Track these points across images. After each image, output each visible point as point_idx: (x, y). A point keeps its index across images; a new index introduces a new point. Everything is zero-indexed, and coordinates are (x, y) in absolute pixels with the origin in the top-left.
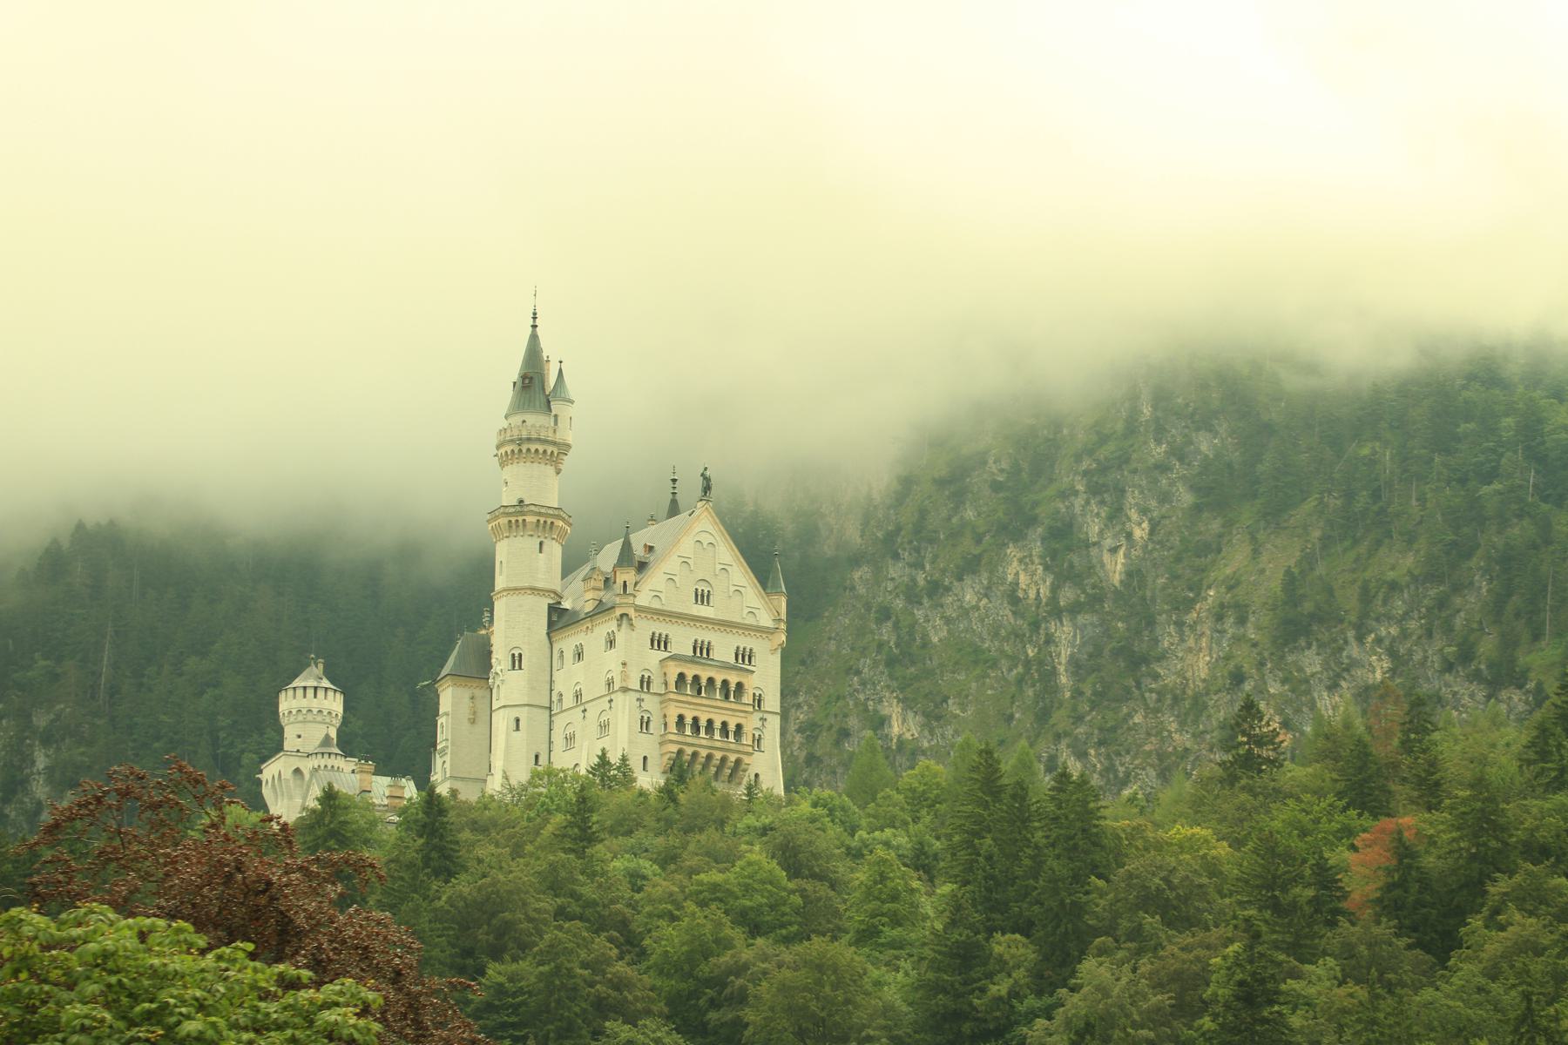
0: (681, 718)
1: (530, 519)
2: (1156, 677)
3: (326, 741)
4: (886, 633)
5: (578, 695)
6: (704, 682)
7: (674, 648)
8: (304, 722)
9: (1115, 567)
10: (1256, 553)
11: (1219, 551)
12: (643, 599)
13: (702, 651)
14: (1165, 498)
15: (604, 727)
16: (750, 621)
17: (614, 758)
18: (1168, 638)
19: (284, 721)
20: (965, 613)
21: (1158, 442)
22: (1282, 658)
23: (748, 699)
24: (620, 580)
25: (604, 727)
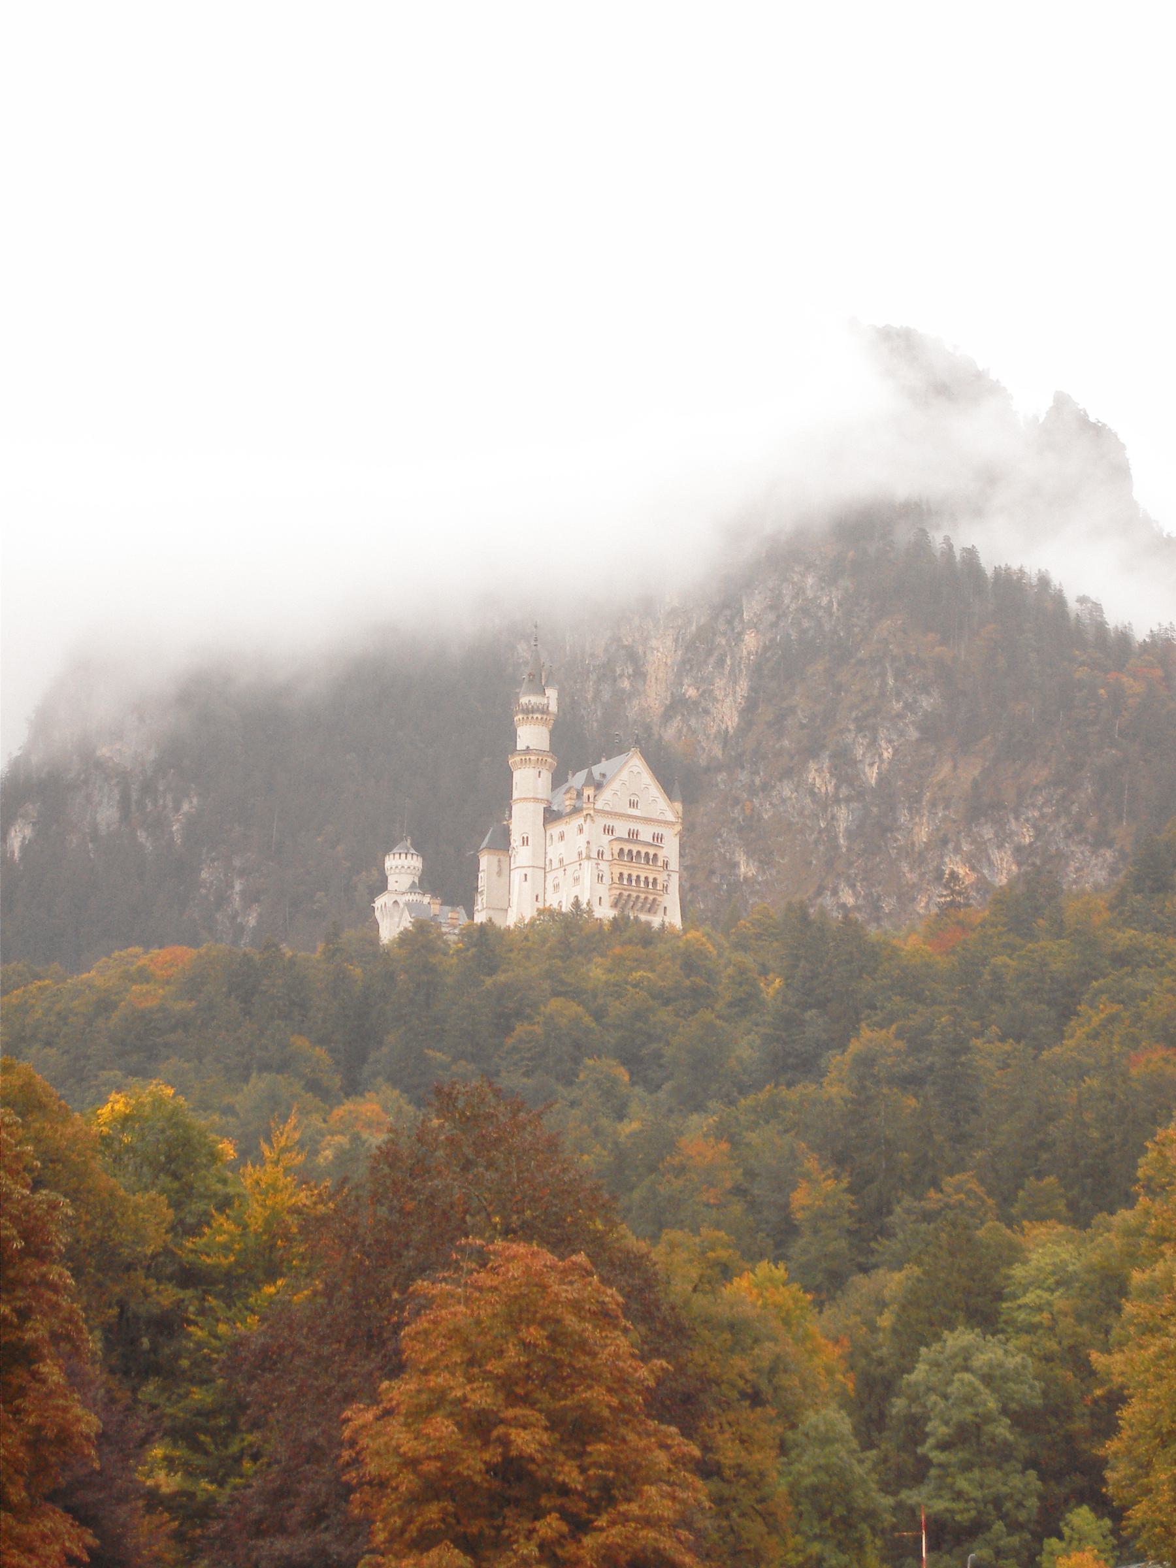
0: (621, 874)
1: (533, 758)
2: (896, 840)
3: (413, 884)
4: (736, 813)
5: (561, 861)
6: (634, 854)
7: (617, 834)
8: (400, 873)
9: (872, 775)
10: (955, 767)
11: (934, 765)
12: (599, 805)
13: (633, 836)
14: (901, 734)
15: (577, 879)
16: (661, 818)
17: (584, 902)
18: (903, 817)
19: (388, 873)
20: (784, 801)
21: (898, 701)
22: (971, 830)
23: (660, 863)
24: (586, 793)
25: (577, 879)
